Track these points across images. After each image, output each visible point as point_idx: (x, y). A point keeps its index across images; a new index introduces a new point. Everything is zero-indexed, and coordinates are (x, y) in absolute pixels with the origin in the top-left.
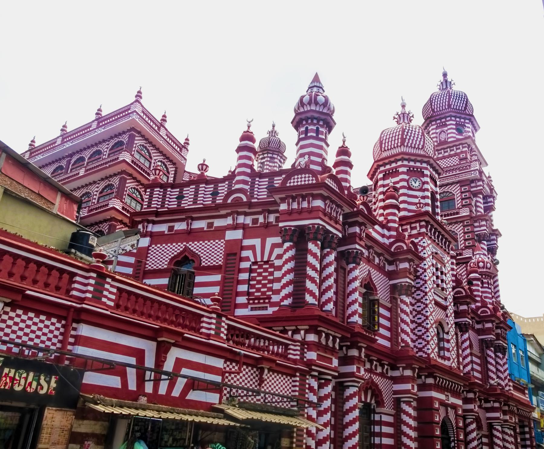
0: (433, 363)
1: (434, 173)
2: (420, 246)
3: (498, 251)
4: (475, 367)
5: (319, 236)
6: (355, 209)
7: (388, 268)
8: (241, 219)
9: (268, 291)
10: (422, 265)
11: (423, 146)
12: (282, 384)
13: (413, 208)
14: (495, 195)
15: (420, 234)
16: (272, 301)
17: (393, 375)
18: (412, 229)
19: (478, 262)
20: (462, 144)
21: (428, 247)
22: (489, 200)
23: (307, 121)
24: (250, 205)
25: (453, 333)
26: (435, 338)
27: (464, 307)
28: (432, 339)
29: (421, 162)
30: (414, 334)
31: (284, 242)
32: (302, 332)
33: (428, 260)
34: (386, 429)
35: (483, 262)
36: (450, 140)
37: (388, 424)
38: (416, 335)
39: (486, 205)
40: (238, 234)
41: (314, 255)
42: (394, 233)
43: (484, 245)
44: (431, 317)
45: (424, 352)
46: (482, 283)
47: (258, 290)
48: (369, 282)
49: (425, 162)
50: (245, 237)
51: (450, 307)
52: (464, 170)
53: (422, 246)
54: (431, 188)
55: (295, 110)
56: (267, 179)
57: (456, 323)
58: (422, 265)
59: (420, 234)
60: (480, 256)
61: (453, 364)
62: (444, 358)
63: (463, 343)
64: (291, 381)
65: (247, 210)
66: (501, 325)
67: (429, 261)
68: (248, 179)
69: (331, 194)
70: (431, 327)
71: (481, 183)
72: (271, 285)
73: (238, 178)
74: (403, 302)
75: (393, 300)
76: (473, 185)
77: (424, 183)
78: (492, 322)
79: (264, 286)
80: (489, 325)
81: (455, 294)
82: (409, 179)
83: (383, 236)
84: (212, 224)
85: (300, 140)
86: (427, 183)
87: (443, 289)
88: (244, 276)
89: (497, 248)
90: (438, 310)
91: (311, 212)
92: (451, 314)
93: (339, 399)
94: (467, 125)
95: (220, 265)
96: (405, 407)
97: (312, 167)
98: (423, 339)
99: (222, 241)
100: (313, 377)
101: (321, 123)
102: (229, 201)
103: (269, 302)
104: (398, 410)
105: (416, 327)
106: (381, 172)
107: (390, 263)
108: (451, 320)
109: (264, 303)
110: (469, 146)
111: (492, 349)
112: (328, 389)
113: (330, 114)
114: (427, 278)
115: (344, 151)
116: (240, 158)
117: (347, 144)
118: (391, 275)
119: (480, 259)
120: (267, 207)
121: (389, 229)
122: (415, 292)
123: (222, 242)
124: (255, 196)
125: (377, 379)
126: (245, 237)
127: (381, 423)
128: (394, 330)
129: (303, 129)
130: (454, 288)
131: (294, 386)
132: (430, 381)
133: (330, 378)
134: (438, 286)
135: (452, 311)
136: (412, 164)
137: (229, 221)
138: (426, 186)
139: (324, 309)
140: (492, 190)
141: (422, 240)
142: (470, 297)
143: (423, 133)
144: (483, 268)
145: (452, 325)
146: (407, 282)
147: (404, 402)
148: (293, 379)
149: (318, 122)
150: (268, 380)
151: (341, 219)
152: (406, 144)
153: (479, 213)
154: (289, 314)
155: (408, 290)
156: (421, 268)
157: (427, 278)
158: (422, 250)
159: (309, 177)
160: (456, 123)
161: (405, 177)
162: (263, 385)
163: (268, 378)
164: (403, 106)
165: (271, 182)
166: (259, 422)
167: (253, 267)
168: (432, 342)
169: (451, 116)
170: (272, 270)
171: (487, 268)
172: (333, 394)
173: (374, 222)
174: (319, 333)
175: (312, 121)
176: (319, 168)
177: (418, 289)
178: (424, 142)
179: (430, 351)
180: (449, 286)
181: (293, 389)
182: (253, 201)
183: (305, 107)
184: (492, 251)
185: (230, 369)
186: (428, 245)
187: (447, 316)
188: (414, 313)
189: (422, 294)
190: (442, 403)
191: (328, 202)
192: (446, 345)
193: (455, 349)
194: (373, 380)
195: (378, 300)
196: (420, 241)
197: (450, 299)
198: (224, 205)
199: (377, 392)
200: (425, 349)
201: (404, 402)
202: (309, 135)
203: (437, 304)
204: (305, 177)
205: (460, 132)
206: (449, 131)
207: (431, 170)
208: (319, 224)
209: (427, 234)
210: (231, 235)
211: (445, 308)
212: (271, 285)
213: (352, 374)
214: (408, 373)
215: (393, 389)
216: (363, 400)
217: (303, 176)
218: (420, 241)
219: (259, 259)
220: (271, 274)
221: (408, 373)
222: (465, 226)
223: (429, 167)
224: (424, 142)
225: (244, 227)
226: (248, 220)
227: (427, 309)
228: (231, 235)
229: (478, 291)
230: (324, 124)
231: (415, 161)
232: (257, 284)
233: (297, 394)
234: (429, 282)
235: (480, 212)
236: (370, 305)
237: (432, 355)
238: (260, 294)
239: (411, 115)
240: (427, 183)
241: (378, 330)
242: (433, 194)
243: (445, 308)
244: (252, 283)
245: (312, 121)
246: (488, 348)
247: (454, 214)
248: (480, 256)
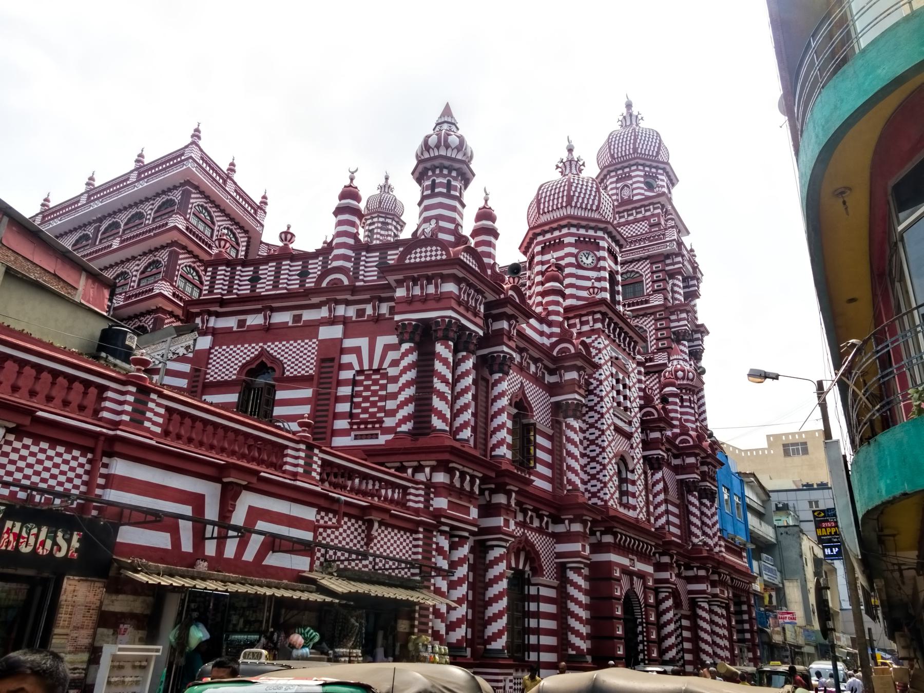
0: (612, 513)
1: (613, 244)
2: (594, 347)
3: (705, 356)
4: (672, 518)
5: (451, 334)
6: (502, 296)
7: (549, 379)
8: (341, 310)
10: (596, 375)
11: (598, 207)
12: (398, 543)
13: (584, 294)
14: (700, 276)
15: (593, 331)
16: (384, 425)
17: (556, 531)
18: (583, 323)
19: (676, 371)
20: (653, 204)
21: (605, 350)
22: (691, 283)
23: (434, 172)
24: (353, 290)
25: (640, 471)
26: (615, 478)
27: (657, 435)
28: (611, 480)
29: (596, 229)
30: (586, 472)
31: (401, 342)
32: (427, 470)
33: (605, 367)
34: (545, 608)
35: (683, 371)
36: (635, 198)
37: (548, 600)
38: (589, 474)
39: (687, 290)
40: (336, 332)
41: (445, 361)
42: (557, 330)
43: (685, 347)
44: (609, 449)
45: (599, 498)
46: (682, 400)
47: (365, 410)
48: (521, 399)
49: (601, 229)
50: (346, 335)
51: (636, 435)
52: (656, 240)
53: (596, 348)
54: (610, 266)
55: (417, 156)
57: (644, 457)
58: (596, 375)
59: (593, 331)
60: (679, 363)
61: (641, 516)
62: (627, 506)
63: (654, 485)
64: (411, 538)
65: (349, 297)
66: (709, 460)
67: (607, 370)
68: (350, 253)
69: (468, 275)
70: (610, 462)
71: (680, 259)
72: (383, 404)
73: (336, 252)
74: (569, 426)
75: (556, 424)
76: (668, 261)
77: (599, 259)
78: (696, 455)
79: (374, 404)
80: (691, 460)
81: (644, 415)
82: (578, 253)
83: (542, 334)
84: (300, 316)
85: (424, 198)
86: (604, 259)
87: (626, 409)
88: (345, 391)
89: (703, 352)
91: (440, 300)
92: (638, 444)
93: (480, 565)
94: (660, 177)
95: (311, 376)
96: (572, 575)
97: (441, 236)
98: (598, 480)
99: (314, 340)
100: (443, 533)
101: (454, 174)
102: (324, 285)
103: (381, 427)
104: (563, 581)
105: (589, 463)
106: (538, 244)
107: (552, 372)
108: (638, 453)
109: (374, 428)
110: (663, 206)
111: (696, 494)
112: (464, 551)
113: (467, 163)
114: (604, 393)
115: (486, 214)
116: (339, 223)
117: (490, 204)
118: (552, 389)
119: (679, 366)
120: (379, 293)
121: (550, 324)
122: (587, 412)
124: (361, 277)
125: (532, 537)
126: (346, 335)
127: (538, 599)
128: (557, 466)
129: (428, 183)
130: (641, 408)
131: (415, 546)
132: (608, 539)
133: (466, 534)
134: (619, 404)
135: (638, 440)
136: (582, 231)
137: (324, 312)
138: (602, 263)
139: (458, 437)
140: (695, 268)
141: (596, 339)
142: (665, 421)
143: (597, 189)
144: (683, 378)
145: (639, 460)
146: (575, 399)
147: (572, 569)
148: (414, 536)
149: (450, 172)
150: (379, 538)
151: (482, 310)
152: (573, 204)
153: (677, 302)
154: (408, 443)
155: (577, 411)
156: (595, 379)
157: (604, 393)
158: (597, 354)
159: (436, 250)
160: (645, 175)
161: (573, 250)
162: (372, 545)
163: (379, 534)
164: (570, 150)
165: (383, 257)
166: (366, 596)
167: (358, 378)
168: (611, 484)
169: (637, 164)
170: (385, 382)
171: (688, 379)
172: (471, 557)
173: (528, 314)
174: (450, 472)
175: (441, 171)
176: (451, 238)
177: (591, 409)
178: (599, 201)
179: (608, 497)
180: (634, 405)
181: (413, 550)
182: (358, 284)
183: (431, 151)
184: (696, 355)
185: (326, 522)
186: (605, 347)
187: (632, 447)
188: (586, 443)
189: (597, 416)
190: (625, 571)
191: (463, 285)
192: (631, 488)
193: (643, 493)
194: (527, 537)
195: (534, 424)
196: (593, 341)
197: (636, 422)
198: (317, 291)
199: (533, 555)
200: (601, 494)
201: (572, 569)
202: (437, 190)
203: (618, 430)
204: (431, 251)
205: (650, 187)
206: (635, 186)
207: (610, 240)
208: (450, 317)
209: (604, 331)
210: (326, 333)
211: (629, 436)
212: (383, 404)
213: (497, 530)
214: (577, 527)
215: (556, 550)
216: (513, 565)
217: (429, 248)
218: (593, 341)
219: (366, 367)
220: (384, 387)
221: (577, 527)
222: (656, 320)
223: (606, 236)
224: (599, 201)
225: (345, 321)
226: (351, 312)
227: (604, 437)
228: (326, 333)
229: (676, 411)
230: (458, 175)
231: (587, 228)
233: (420, 557)
234: (606, 399)
235: (679, 300)
236: (523, 432)
237: (611, 503)
238: (367, 416)
239: (581, 163)
240: (604, 259)
241: (535, 466)
242: (612, 274)
243: (629, 436)
244: (356, 400)
245: (441, 171)
246: (690, 492)
247: (642, 303)
248: (679, 363)
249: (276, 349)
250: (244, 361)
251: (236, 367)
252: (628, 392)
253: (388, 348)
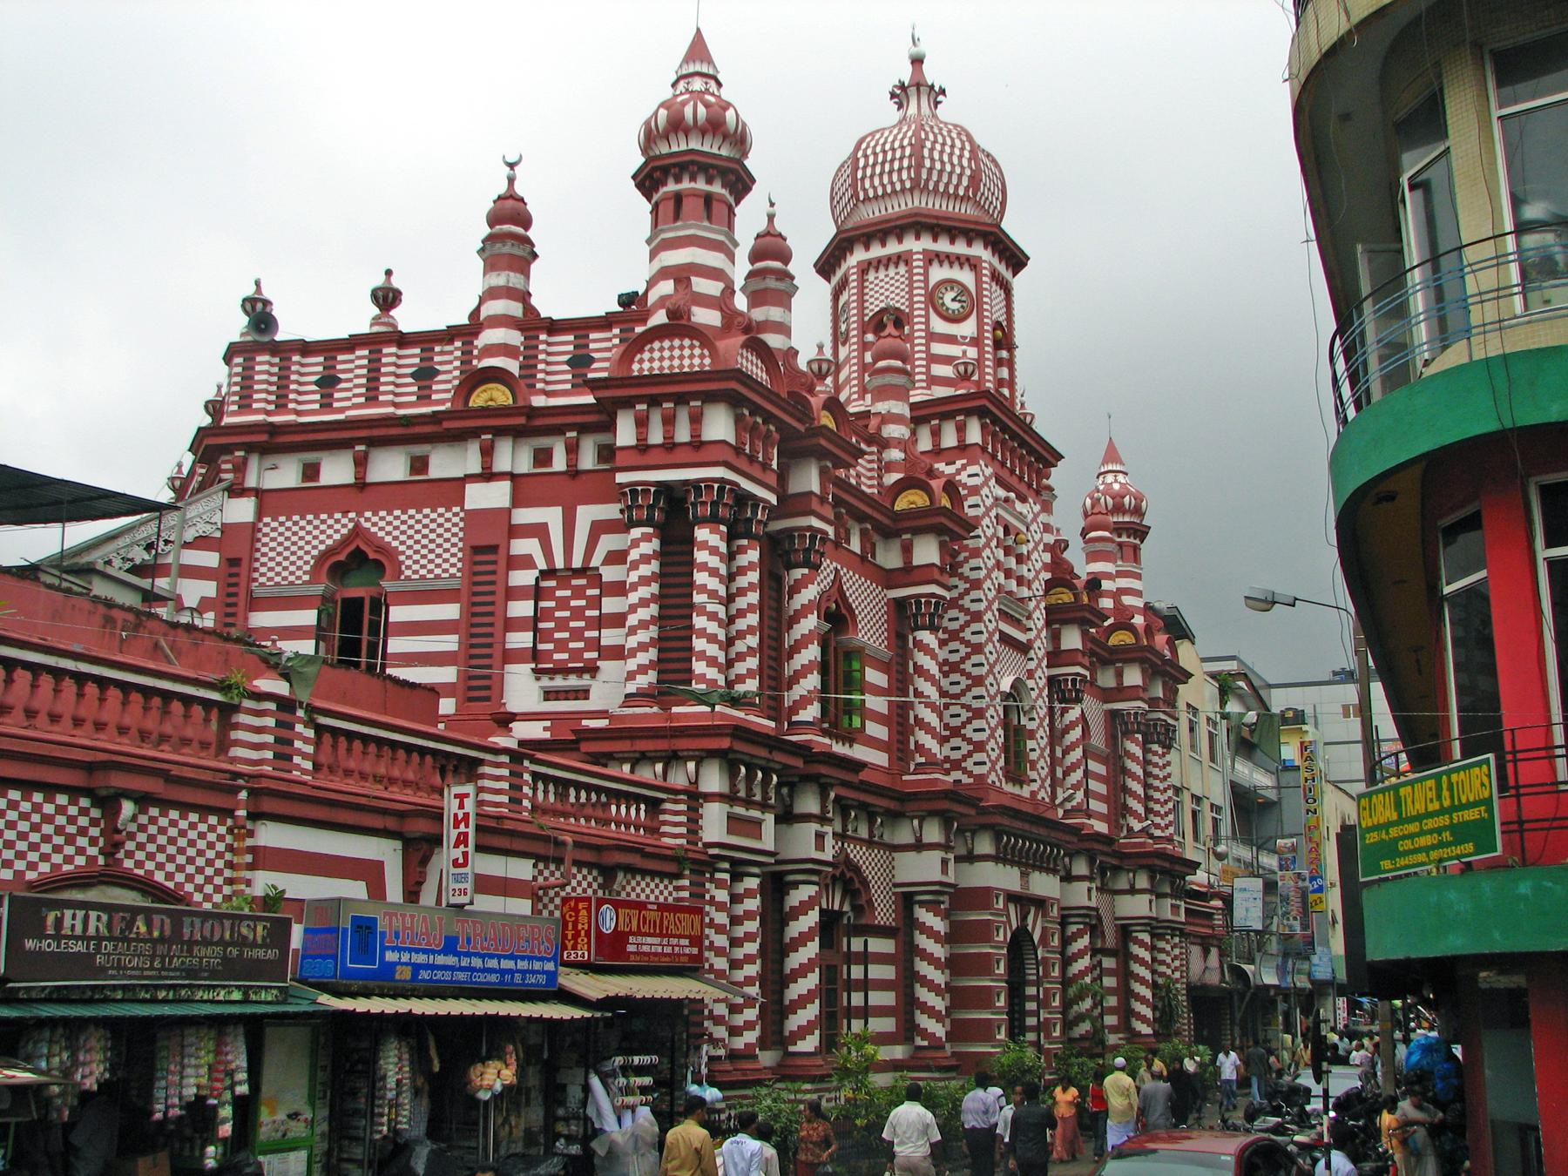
0: (992, 800)
47: (561, 646)
50: (518, 500)
51: (1037, 644)
72: (595, 634)
74: (919, 645)
79: (577, 634)
88: (522, 609)
95: (455, 584)
99: (456, 509)
111: (1139, 737)
123: (456, 515)
125: (856, 853)
126: (518, 500)
167: (544, 584)
170: (596, 592)
194: (847, 855)
199: (857, 885)
201: (922, 904)
211: (1024, 648)
212: (595, 634)
220: (596, 603)
232: (558, 629)
237: (992, 777)
238: (565, 656)
243: (1024, 648)
244: (542, 625)
246: (1127, 734)
249: (382, 524)
250: (322, 547)
251: (307, 558)
252: (1024, 570)
253: (598, 529)
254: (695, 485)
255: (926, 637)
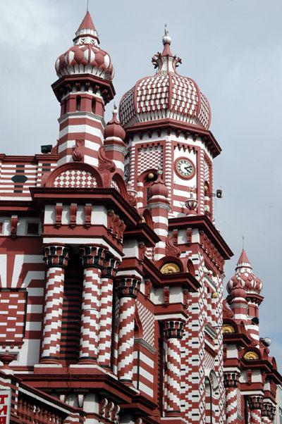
9: (17, 332)
56: (15, 166)
90: (208, 356)
203: (208, 349)
211: (213, 354)
243: (213, 354)
246: (253, 409)
254: (87, 246)
255: (175, 341)
